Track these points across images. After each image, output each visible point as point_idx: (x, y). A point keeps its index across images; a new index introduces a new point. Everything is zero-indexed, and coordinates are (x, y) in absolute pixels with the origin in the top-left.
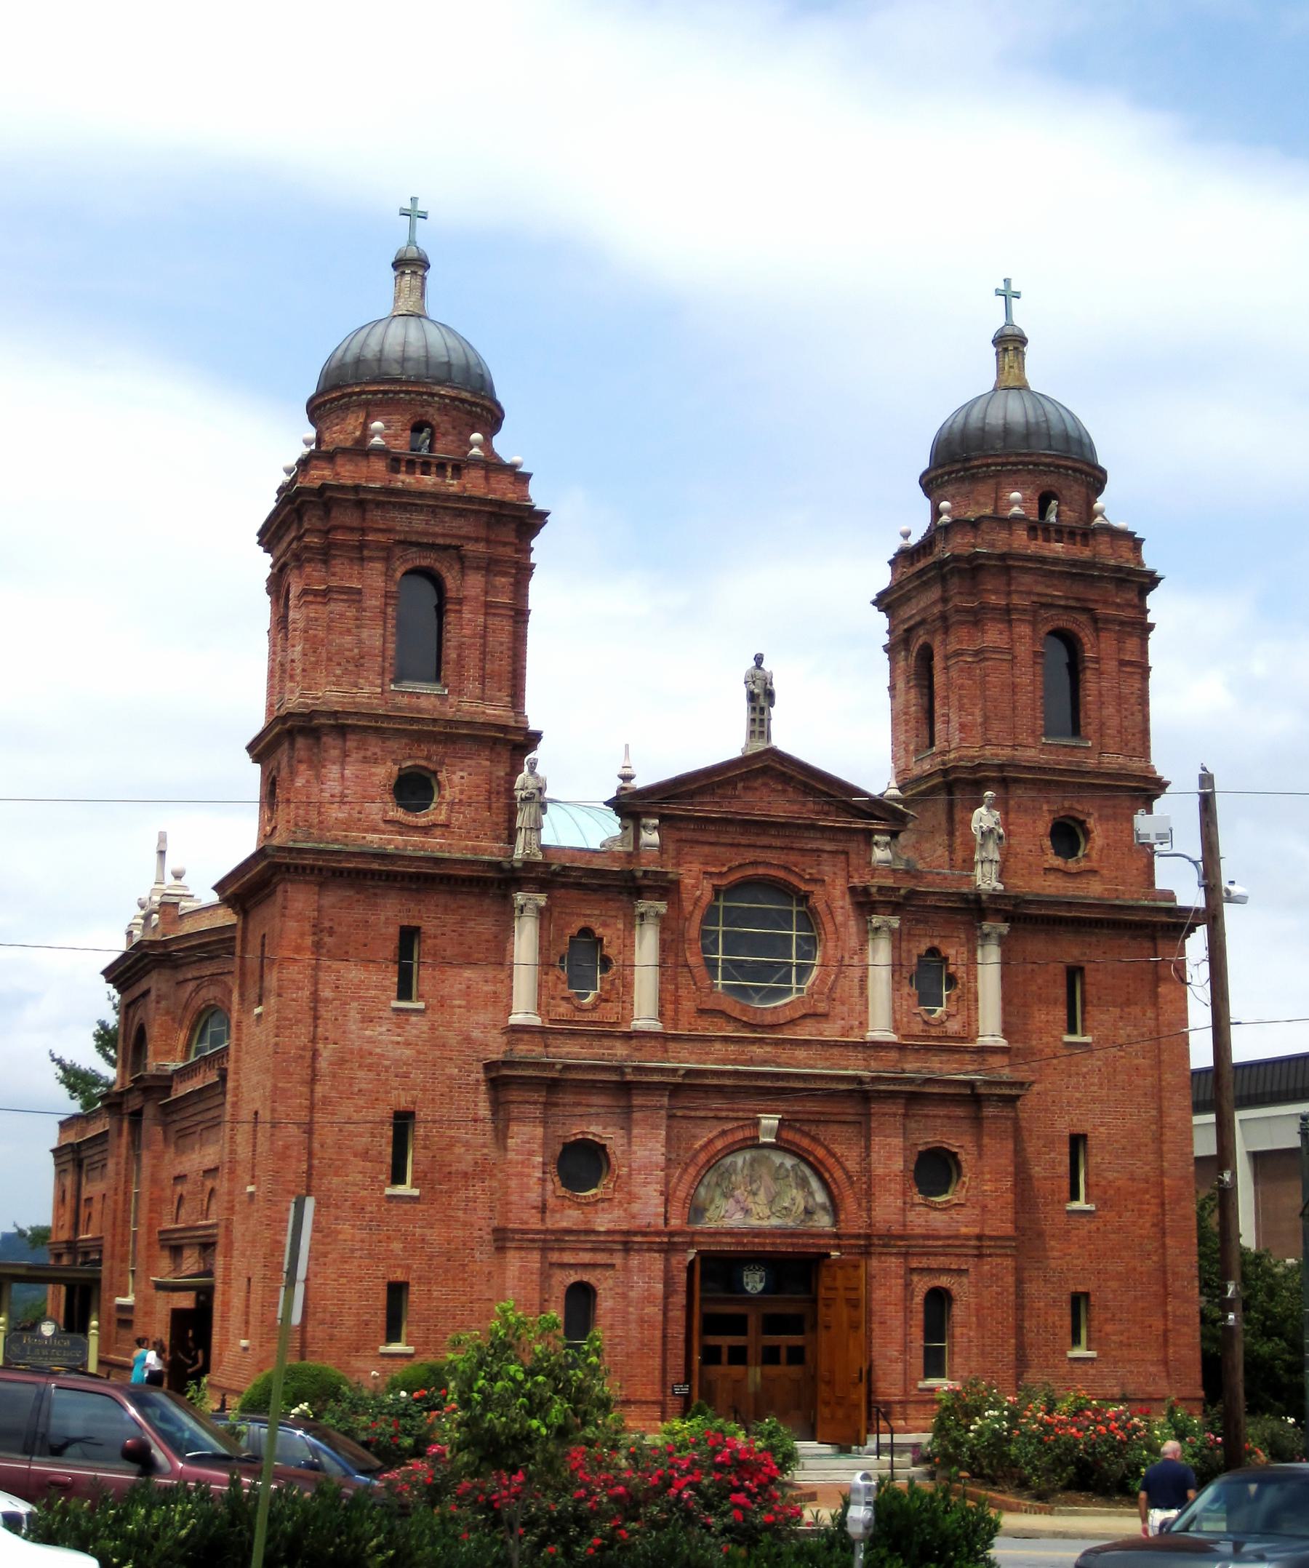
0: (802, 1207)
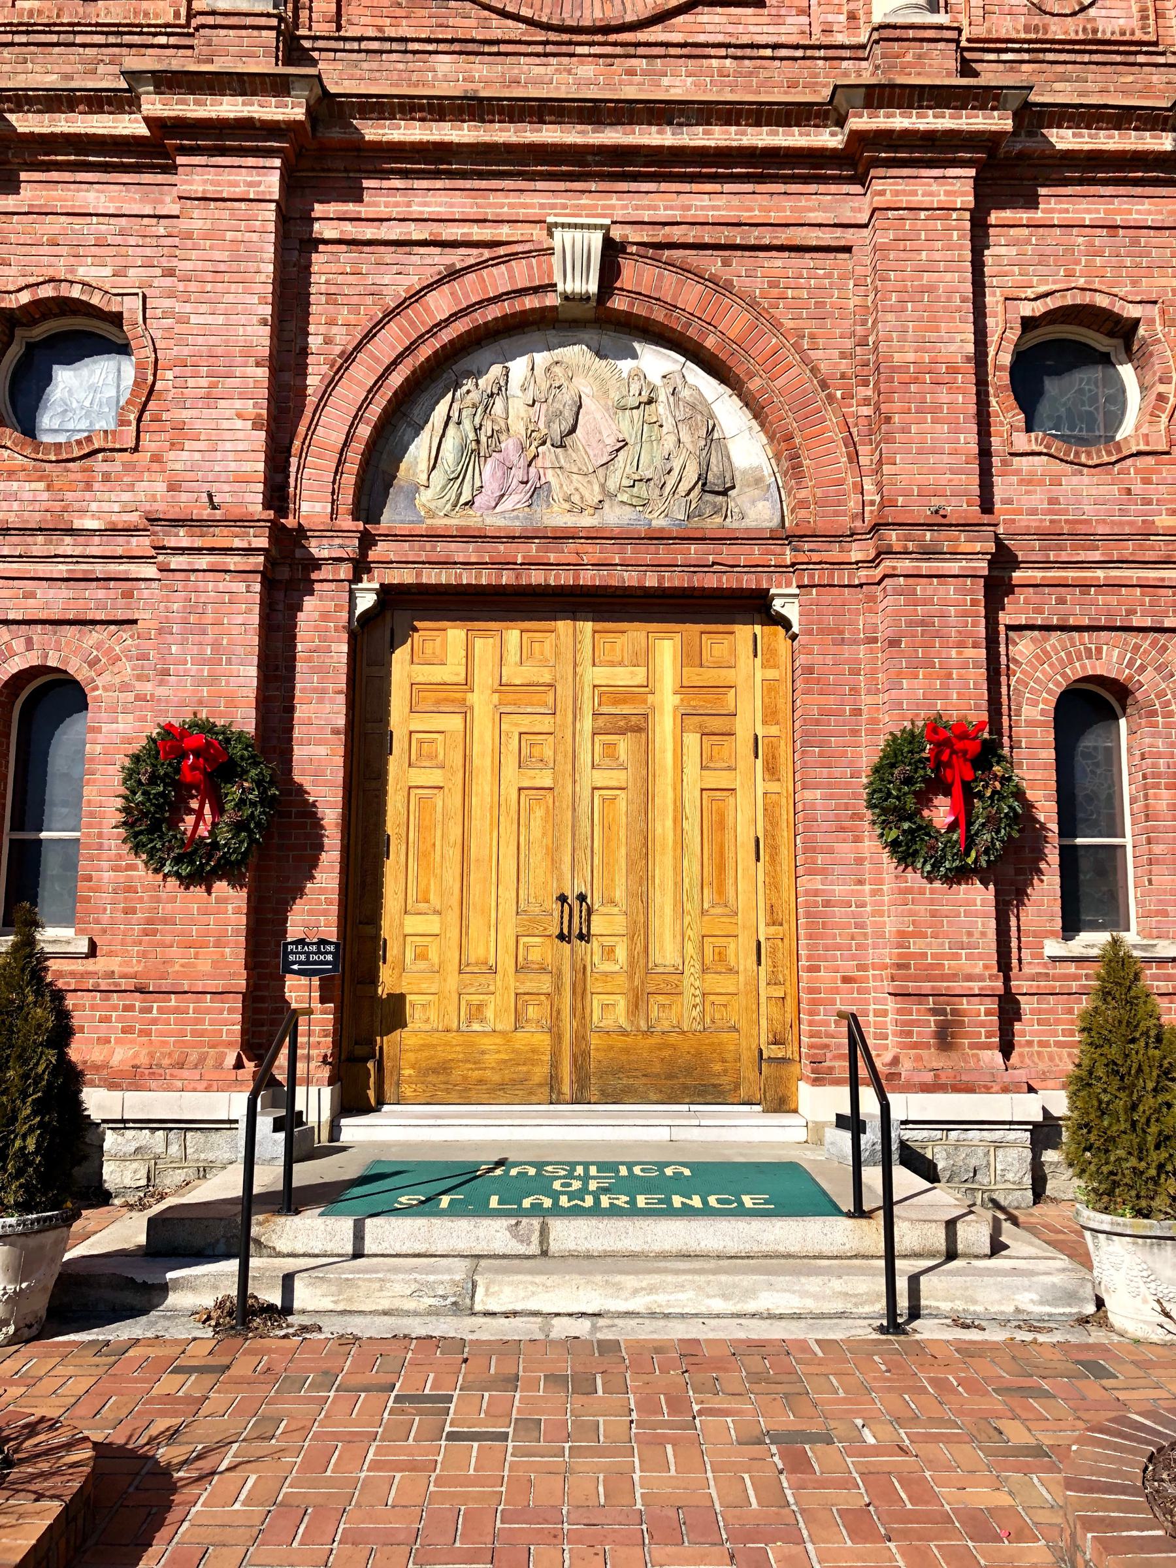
0: (691, 475)
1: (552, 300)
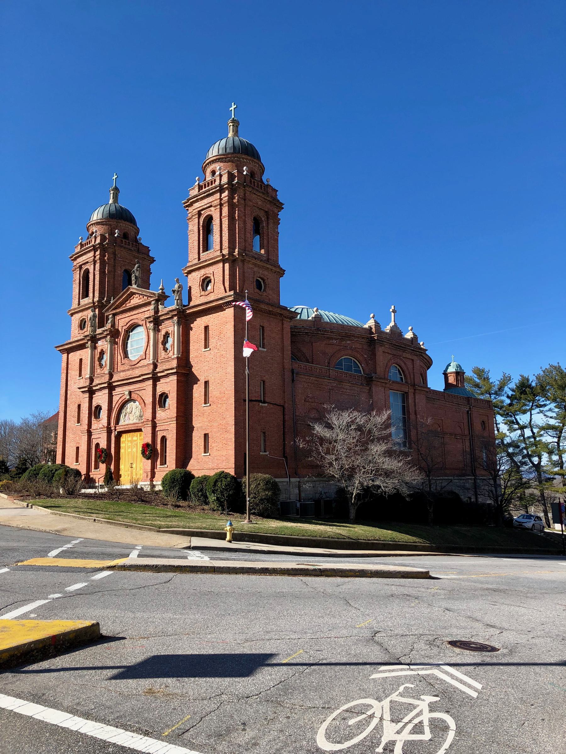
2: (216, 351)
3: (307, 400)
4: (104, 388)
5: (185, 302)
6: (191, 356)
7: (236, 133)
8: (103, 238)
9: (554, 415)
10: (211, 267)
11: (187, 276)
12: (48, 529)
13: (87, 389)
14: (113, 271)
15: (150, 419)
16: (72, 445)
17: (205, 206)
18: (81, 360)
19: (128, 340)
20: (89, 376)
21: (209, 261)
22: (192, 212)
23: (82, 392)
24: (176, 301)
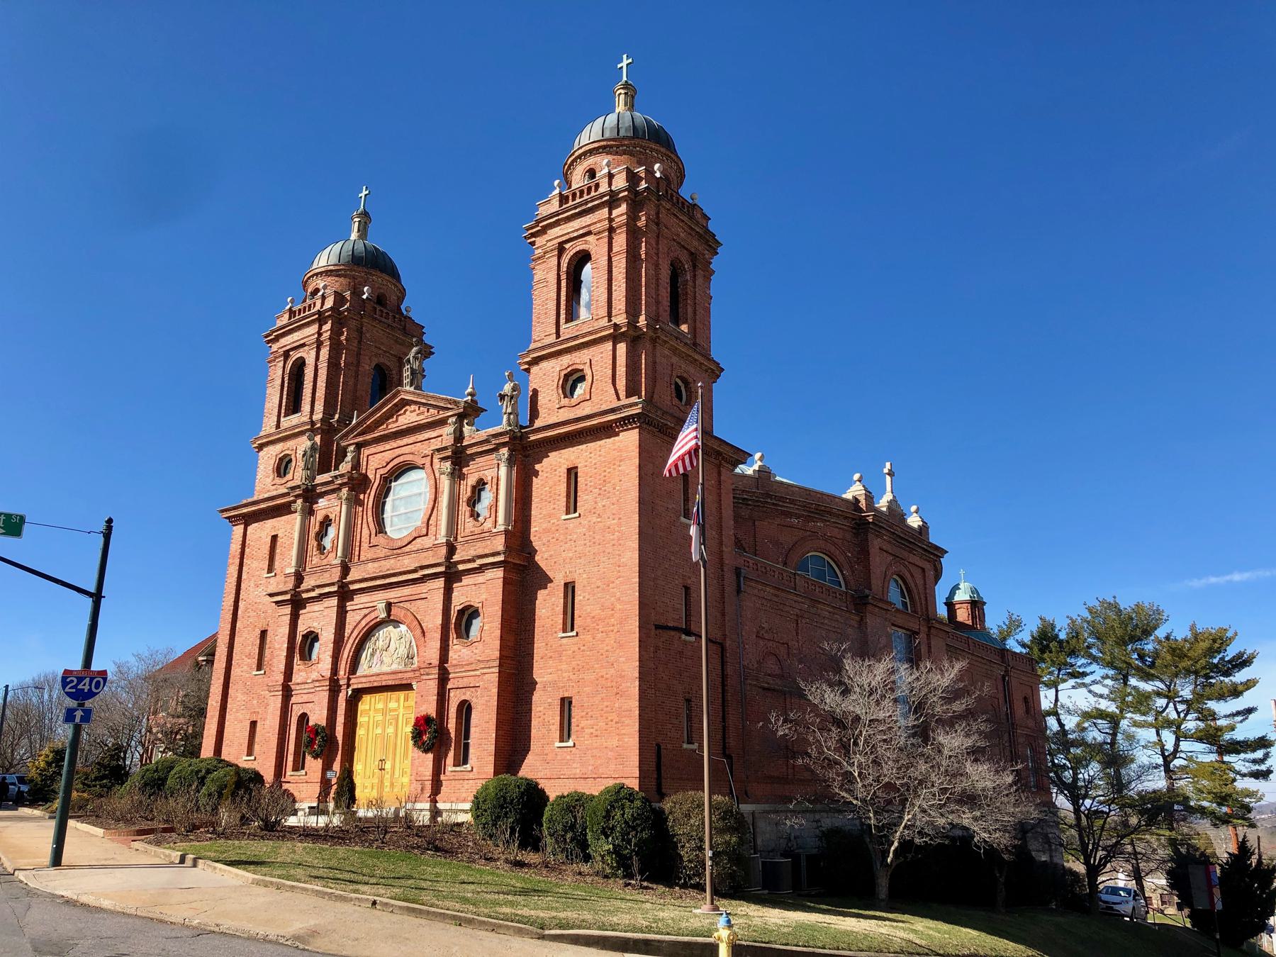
0: (406, 656)
1: (378, 620)
2: (594, 519)
3: (761, 635)
4: (328, 595)
5: (525, 421)
6: (533, 530)
7: (631, 106)
8: (339, 298)
9: (1105, 691)
10: (585, 351)
11: (528, 371)
12: (272, 933)
13: (288, 597)
14: (355, 364)
15: (436, 662)
16: (241, 717)
17: (575, 234)
18: (274, 538)
19: (386, 496)
20: (293, 570)
21: (583, 337)
22: (545, 245)
23: (277, 603)
24: (505, 417)
